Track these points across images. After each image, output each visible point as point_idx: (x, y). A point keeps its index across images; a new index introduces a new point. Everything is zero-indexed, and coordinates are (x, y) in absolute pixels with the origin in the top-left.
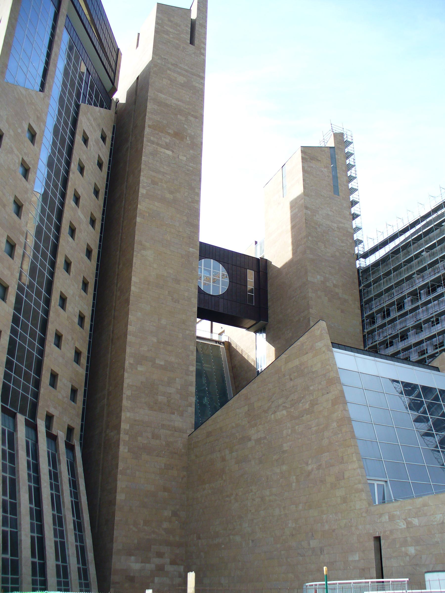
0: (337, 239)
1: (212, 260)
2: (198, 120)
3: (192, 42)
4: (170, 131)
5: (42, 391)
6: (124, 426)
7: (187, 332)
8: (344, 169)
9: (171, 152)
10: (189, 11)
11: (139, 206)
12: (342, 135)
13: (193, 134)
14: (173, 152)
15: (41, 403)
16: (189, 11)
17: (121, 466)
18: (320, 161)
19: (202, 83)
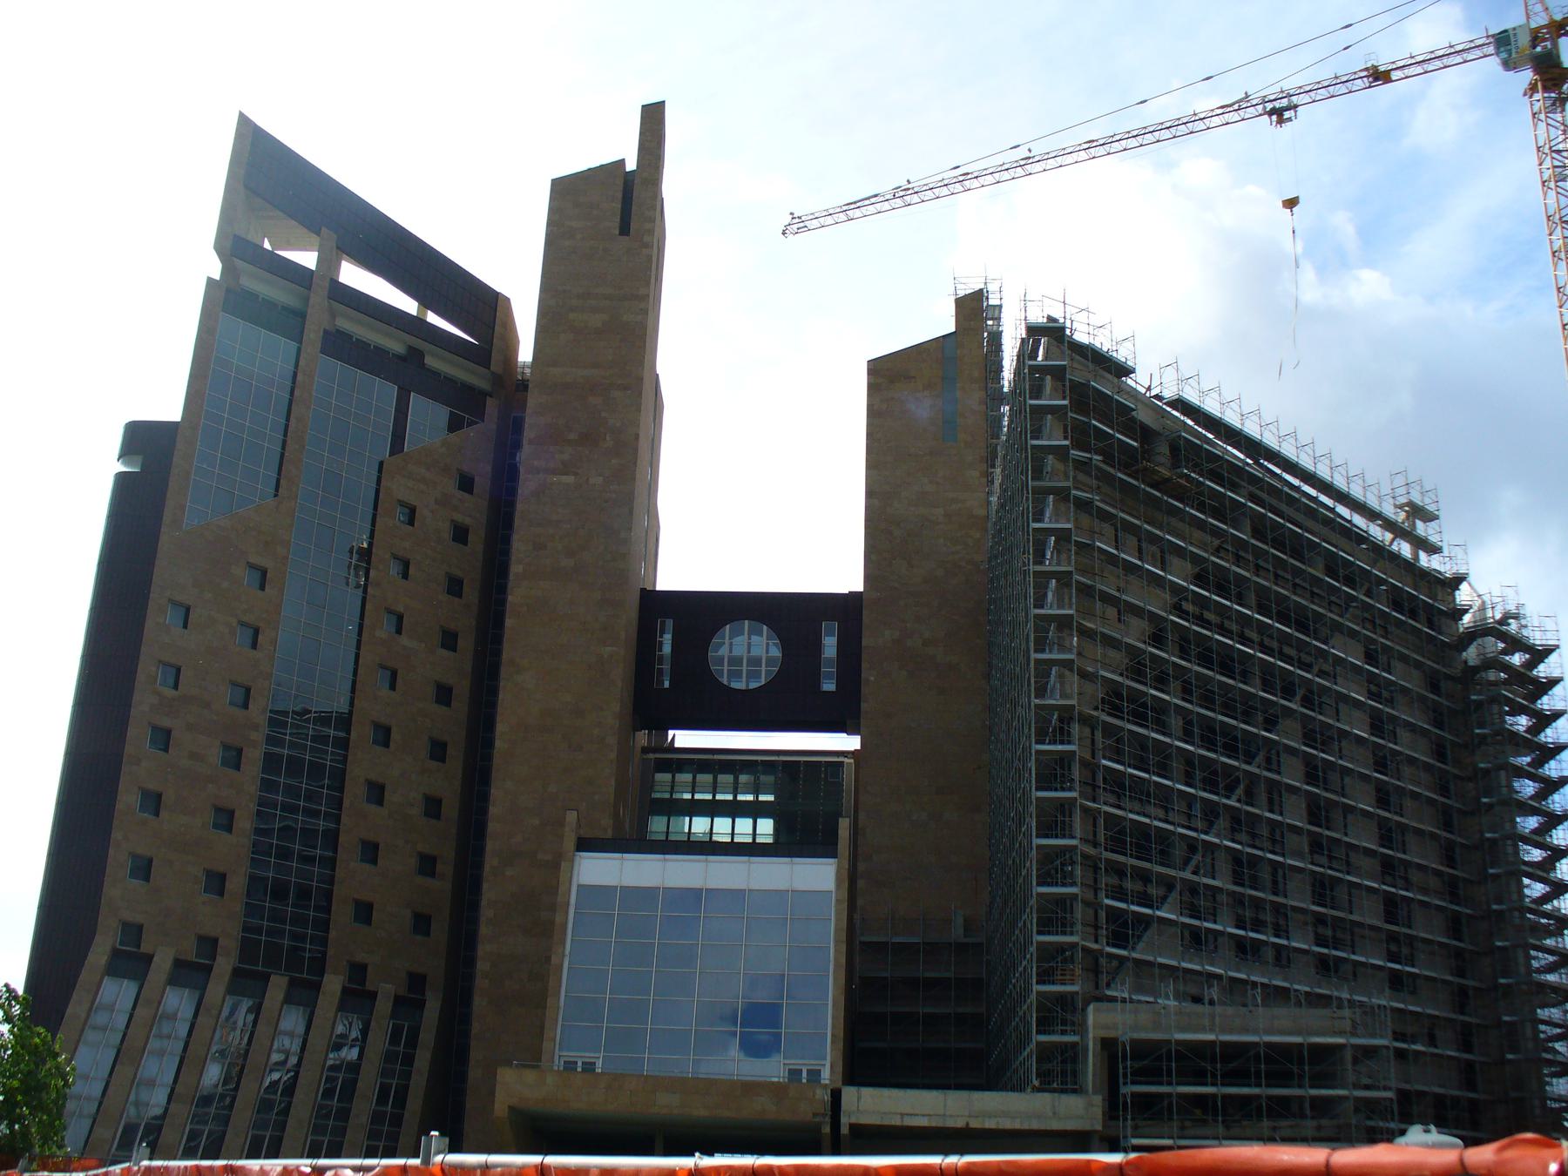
0: (942, 540)
1: (746, 622)
2: (629, 392)
3: (625, 229)
4: (572, 436)
5: (333, 934)
6: (482, 966)
7: (596, 797)
8: (976, 374)
9: (573, 477)
10: (622, 163)
11: (510, 598)
12: (979, 296)
13: (618, 425)
14: (576, 474)
15: (331, 952)
16: (622, 163)
17: (476, 1027)
18: (914, 377)
19: (642, 309)
